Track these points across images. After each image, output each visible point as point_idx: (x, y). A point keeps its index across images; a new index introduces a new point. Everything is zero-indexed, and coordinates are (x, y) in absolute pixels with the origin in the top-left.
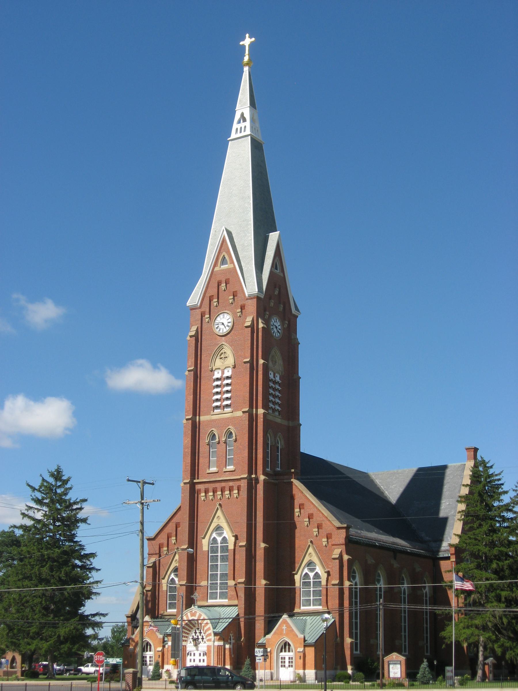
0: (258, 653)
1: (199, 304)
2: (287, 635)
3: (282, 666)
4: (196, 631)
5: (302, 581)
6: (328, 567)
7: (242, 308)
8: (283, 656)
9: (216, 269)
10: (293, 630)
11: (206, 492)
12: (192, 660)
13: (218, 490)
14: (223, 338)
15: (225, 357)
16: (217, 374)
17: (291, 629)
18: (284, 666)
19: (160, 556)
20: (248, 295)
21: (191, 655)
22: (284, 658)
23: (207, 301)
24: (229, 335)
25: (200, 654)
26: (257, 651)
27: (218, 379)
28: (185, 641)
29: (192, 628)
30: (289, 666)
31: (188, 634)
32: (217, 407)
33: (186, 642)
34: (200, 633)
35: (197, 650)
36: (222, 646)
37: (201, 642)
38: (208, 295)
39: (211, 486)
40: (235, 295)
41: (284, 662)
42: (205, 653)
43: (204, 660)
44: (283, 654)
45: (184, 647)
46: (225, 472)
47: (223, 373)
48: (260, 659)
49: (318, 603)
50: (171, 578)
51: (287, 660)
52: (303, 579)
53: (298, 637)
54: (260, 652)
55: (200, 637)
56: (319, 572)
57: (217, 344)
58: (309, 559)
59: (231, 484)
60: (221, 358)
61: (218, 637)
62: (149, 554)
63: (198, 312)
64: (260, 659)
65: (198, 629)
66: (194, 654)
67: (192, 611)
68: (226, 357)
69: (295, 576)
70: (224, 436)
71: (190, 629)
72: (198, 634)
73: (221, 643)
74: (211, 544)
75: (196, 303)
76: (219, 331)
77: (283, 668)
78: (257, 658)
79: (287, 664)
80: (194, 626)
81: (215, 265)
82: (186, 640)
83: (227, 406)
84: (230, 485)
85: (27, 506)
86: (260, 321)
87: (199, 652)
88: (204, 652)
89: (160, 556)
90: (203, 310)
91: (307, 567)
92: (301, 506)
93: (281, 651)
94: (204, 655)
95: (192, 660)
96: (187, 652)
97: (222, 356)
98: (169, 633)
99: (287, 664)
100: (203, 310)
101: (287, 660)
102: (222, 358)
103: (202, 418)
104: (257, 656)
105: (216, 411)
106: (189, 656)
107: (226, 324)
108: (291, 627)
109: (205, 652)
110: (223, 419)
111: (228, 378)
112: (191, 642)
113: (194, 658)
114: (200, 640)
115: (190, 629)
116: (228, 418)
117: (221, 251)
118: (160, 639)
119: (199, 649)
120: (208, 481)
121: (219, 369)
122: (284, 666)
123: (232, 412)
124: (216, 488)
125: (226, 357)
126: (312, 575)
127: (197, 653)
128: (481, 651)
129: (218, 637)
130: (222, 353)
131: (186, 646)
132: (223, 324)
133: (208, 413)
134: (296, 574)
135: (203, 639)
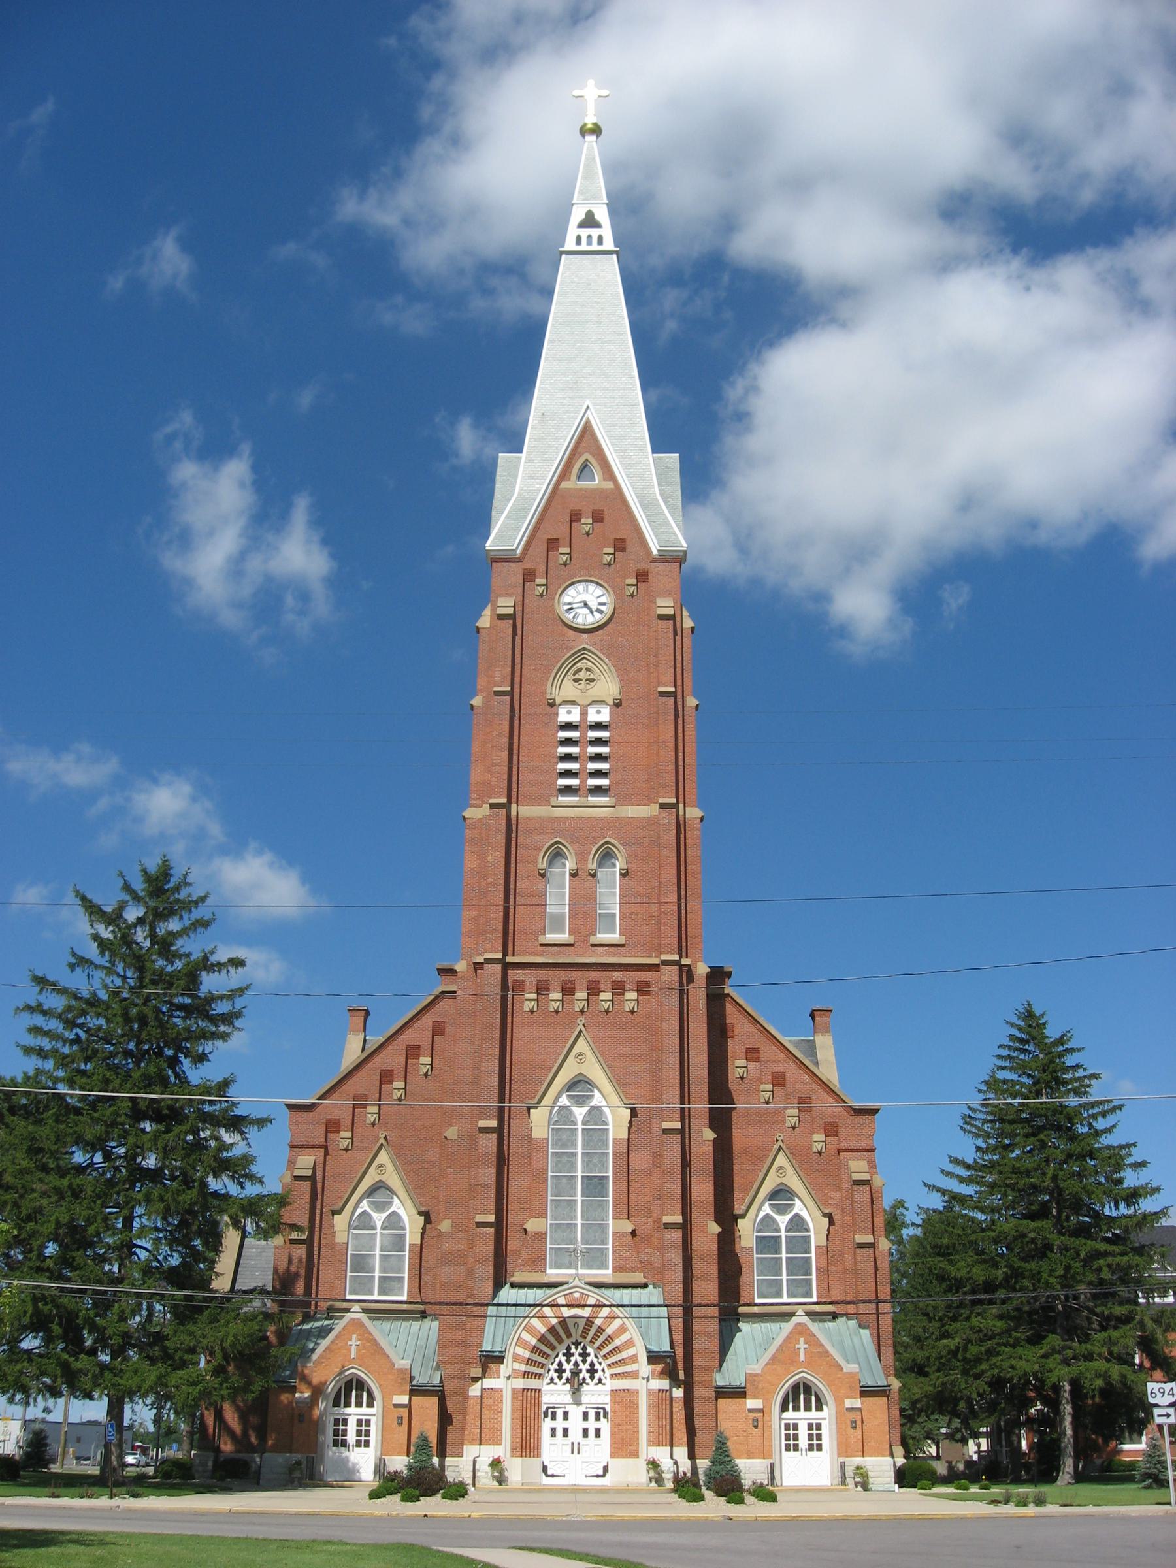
0: (1159, 1395)
1: (518, 552)
2: (809, 1363)
3: (788, 1448)
4: (569, 1348)
5: (755, 1234)
6: (827, 1204)
7: (642, 577)
8: (791, 1422)
9: (565, 485)
10: (827, 1352)
11: (542, 988)
12: (559, 1432)
13: (577, 986)
14: (585, 636)
15: (587, 680)
16: (564, 716)
17: (821, 1350)
18: (796, 1448)
19: (326, 1153)
20: (658, 551)
21: (554, 1418)
22: (796, 1427)
23: (540, 548)
24: (600, 632)
25: (586, 1416)
26: (1156, 1391)
27: (569, 726)
28: (539, 1378)
29: (560, 1341)
30: (811, 1447)
31: (547, 1356)
32: (568, 790)
33: (540, 1380)
34: (584, 1355)
35: (578, 1402)
36: (667, 1390)
37: (588, 1380)
38: (543, 536)
39: (556, 978)
40: (620, 546)
41: (796, 1437)
42: (602, 1411)
43: (598, 1433)
44: (790, 1414)
45: (537, 1394)
46: (593, 946)
47: (584, 713)
48: (1168, 1416)
49: (773, 1290)
50: (359, 1211)
51: (803, 1432)
52: (758, 1232)
53: (842, 1369)
54: (1164, 1393)
55: (584, 1367)
56: (805, 1214)
57: (568, 648)
58: (779, 1181)
59: (617, 975)
60: (576, 680)
61: (660, 1367)
62: (292, 1146)
63: (517, 569)
64: (1168, 1416)
65: (577, 1344)
66: (566, 1415)
67: (571, 1293)
68: (592, 680)
69: (739, 1220)
70: (593, 859)
71: (556, 1343)
72: (576, 1358)
73: (665, 1384)
74: (556, 1123)
75: (514, 547)
76: (574, 618)
77: (792, 1453)
78: (1157, 1411)
79: (803, 1442)
80: (569, 1335)
81: (564, 475)
82: (540, 1375)
83: (597, 790)
84: (614, 979)
85: (74, 954)
86: (685, 613)
87: (583, 1408)
88: (598, 1408)
89: (326, 1153)
90: (529, 566)
91: (769, 1201)
92: (752, 1054)
93: (784, 1408)
94: (598, 1418)
95: (559, 1432)
96: (544, 1408)
97: (581, 675)
98: (497, 1354)
99: (803, 1442)
100: (528, 565)
101: (803, 1432)
102: (581, 680)
103: (524, 811)
104: (1157, 1405)
105: (564, 799)
106: (548, 1420)
107: (593, 605)
108: (822, 1345)
109: (604, 1409)
110: (588, 820)
111: (598, 726)
112: (552, 1380)
113: (566, 1424)
114: (584, 1374)
115: (556, 1343)
116: (602, 819)
117: (579, 451)
118: (401, 1371)
119: (585, 1399)
120: (550, 961)
121: (573, 703)
122: (796, 1448)
123: (614, 807)
124: (572, 982)
125: (592, 680)
126: (783, 1220)
127: (576, 1412)
128: (1069, 1414)
129: (660, 1367)
130: (580, 670)
131: (540, 1390)
132: (586, 605)
133: (542, 801)
134: (743, 1216)
135: (592, 1371)
